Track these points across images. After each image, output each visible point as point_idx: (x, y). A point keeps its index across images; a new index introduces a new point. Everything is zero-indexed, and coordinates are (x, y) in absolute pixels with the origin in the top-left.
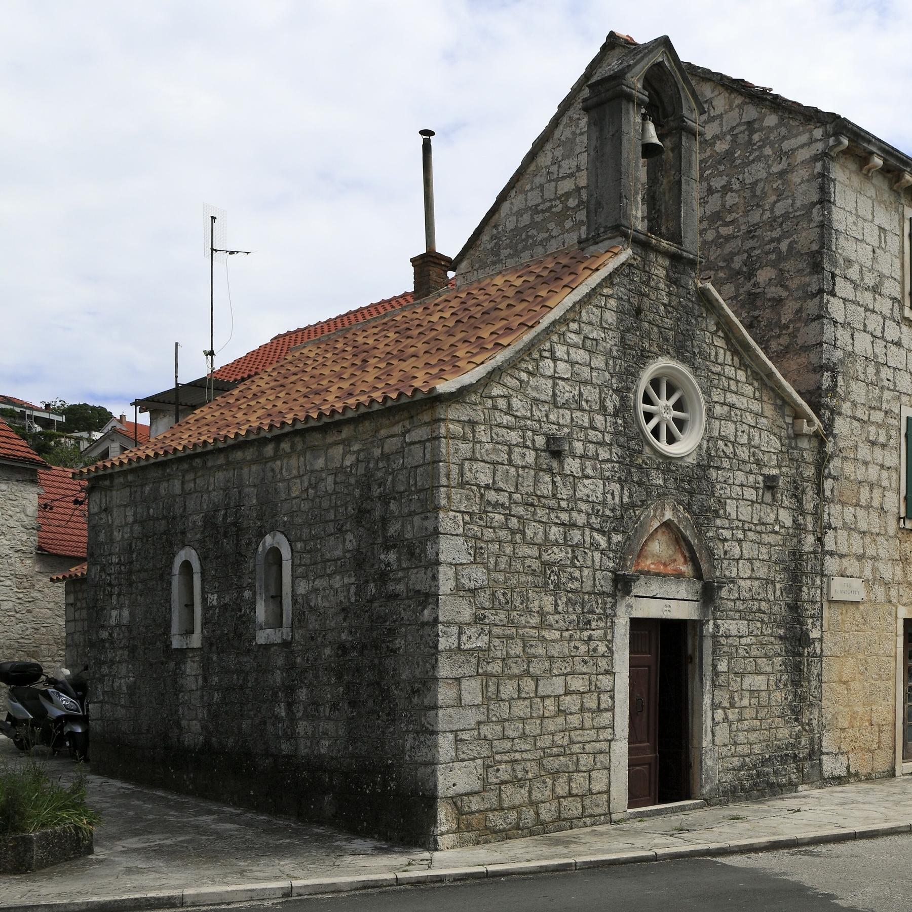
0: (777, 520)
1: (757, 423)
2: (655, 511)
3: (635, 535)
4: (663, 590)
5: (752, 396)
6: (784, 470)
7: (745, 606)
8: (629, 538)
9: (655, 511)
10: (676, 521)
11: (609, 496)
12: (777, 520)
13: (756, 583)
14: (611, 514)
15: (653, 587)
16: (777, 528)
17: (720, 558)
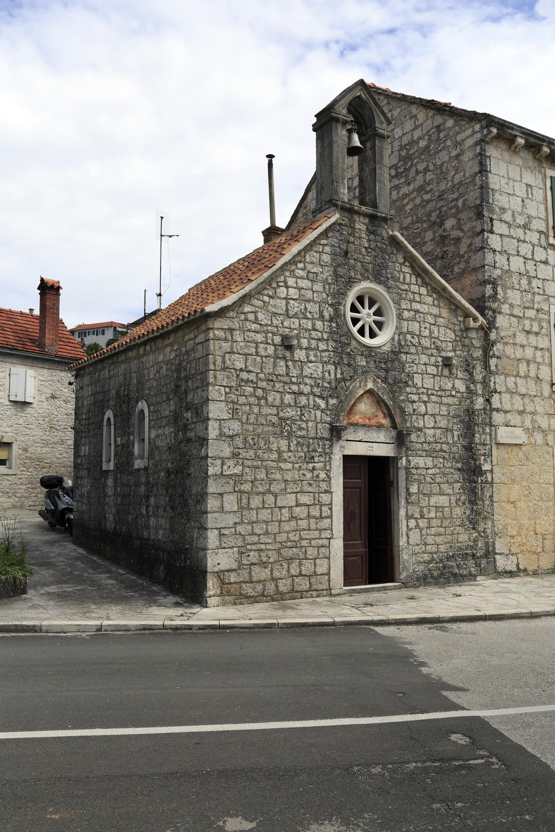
0: (453, 387)
1: (436, 322)
2: (360, 383)
3: (346, 399)
4: (367, 436)
5: (432, 303)
6: (458, 353)
7: (430, 447)
8: (341, 401)
9: (360, 383)
10: (376, 389)
11: (327, 374)
12: (453, 387)
13: (438, 431)
14: (328, 386)
15: (360, 434)
16: (454, 393)
17: (410, 414)
